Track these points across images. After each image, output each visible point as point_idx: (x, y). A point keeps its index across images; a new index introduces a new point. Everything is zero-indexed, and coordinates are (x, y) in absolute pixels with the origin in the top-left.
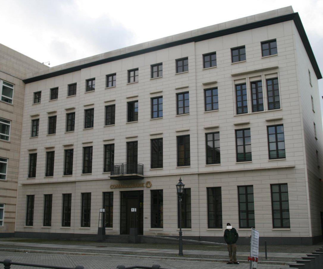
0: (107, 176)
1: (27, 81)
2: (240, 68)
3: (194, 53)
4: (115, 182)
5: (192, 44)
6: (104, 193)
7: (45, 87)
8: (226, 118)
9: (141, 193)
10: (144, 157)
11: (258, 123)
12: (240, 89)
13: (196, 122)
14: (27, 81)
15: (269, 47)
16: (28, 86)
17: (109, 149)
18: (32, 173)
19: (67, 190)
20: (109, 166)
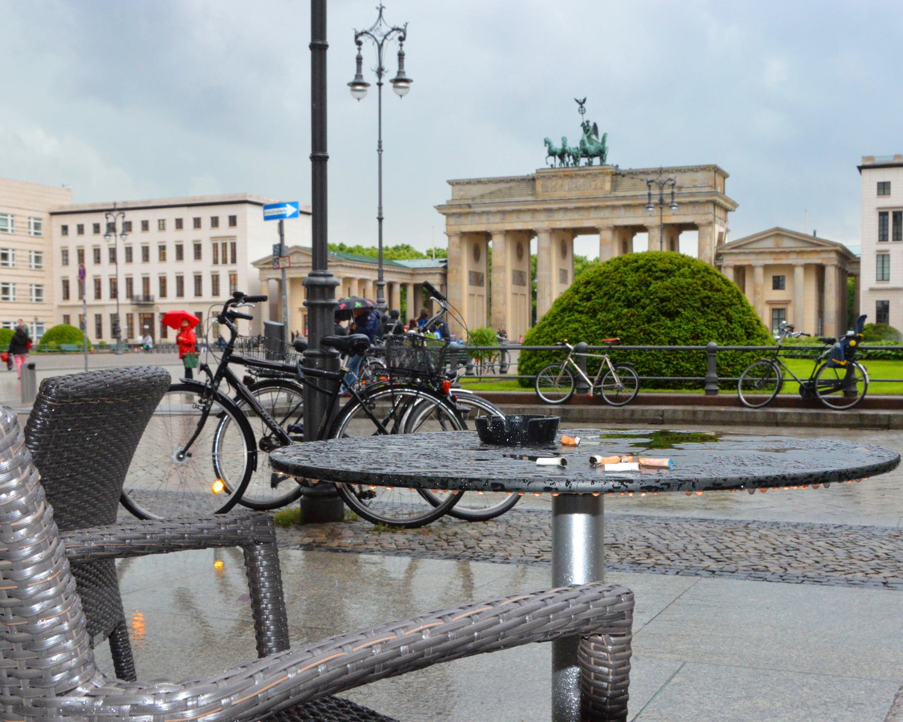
0: (129, 301)
1: (52, 214)
2: (216, 232)
3: (188, 216)
4: (135, 307)
5: (185, 209)
6: (128, 315)
7: (72, 222)
8: (206, 267)
9: (153, 314)
10: (155, 290)
11: (224, 272)
12: (215, 246)
13: (189, 267)
14: (52, 214)
15: (233, 221)
16: (55, 217)
17: (130, 282)
18: (67, 296)
19: (98, 311)
20: (130, 295)
